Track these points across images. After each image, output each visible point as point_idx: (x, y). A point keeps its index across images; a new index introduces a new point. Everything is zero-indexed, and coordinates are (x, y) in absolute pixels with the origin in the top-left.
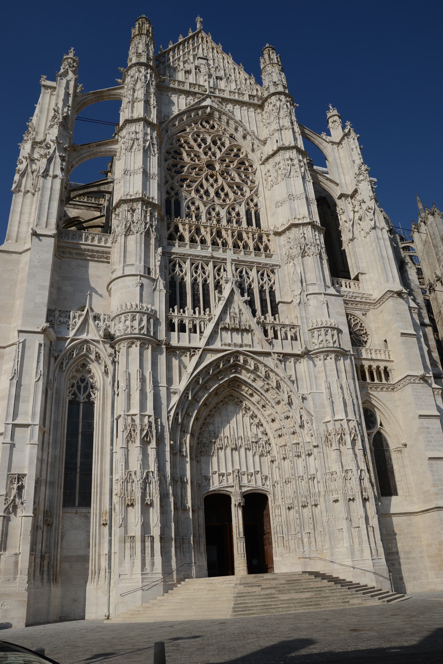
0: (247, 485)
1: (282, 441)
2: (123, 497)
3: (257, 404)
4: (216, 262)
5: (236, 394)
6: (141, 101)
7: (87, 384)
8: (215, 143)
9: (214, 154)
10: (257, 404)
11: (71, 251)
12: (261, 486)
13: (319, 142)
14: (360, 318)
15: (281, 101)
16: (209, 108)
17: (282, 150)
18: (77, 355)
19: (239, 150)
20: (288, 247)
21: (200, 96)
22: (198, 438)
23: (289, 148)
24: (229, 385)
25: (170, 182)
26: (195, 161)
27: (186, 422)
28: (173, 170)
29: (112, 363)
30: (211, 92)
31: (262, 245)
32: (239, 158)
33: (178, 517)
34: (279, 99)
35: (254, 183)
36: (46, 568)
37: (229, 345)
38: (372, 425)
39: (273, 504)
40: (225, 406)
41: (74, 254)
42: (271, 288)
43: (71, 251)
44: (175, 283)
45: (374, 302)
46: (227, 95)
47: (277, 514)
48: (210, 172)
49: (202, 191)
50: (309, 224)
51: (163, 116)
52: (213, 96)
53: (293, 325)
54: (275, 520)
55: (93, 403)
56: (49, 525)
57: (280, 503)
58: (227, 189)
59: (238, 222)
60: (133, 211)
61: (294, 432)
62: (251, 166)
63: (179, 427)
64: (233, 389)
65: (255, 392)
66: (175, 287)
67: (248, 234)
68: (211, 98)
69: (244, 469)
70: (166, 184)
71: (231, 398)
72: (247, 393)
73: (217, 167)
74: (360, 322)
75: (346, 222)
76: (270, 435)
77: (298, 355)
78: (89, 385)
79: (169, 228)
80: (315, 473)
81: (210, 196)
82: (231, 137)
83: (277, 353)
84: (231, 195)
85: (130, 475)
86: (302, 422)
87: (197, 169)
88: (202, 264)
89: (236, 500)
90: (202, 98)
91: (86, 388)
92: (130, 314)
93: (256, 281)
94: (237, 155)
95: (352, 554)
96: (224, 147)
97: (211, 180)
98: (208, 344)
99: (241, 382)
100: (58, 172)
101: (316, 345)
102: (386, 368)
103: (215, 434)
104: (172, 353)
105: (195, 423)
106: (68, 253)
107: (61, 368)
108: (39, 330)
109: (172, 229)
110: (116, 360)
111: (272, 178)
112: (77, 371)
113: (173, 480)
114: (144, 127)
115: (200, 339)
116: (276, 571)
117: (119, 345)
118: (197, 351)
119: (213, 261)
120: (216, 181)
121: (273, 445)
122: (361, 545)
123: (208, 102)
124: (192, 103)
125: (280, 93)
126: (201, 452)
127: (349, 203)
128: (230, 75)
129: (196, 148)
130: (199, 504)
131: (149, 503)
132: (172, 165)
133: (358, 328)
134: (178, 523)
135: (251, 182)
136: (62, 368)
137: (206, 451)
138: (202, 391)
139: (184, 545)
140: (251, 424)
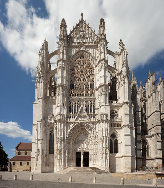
1: (92, 141)
8: (83, 63)
9: (83, 67)
19: (90, 64)
37: (81, 121)
42: (94, 105)
58: (86, 78)
69: (84, 147)
77: (96, 122)
84: (87, 79)
89: (82, 153)
94: (90, 66)
95: (102, 164)
98: (76, 121)
102: (120, 124)
109: (70, 92)
120: (83, 76)
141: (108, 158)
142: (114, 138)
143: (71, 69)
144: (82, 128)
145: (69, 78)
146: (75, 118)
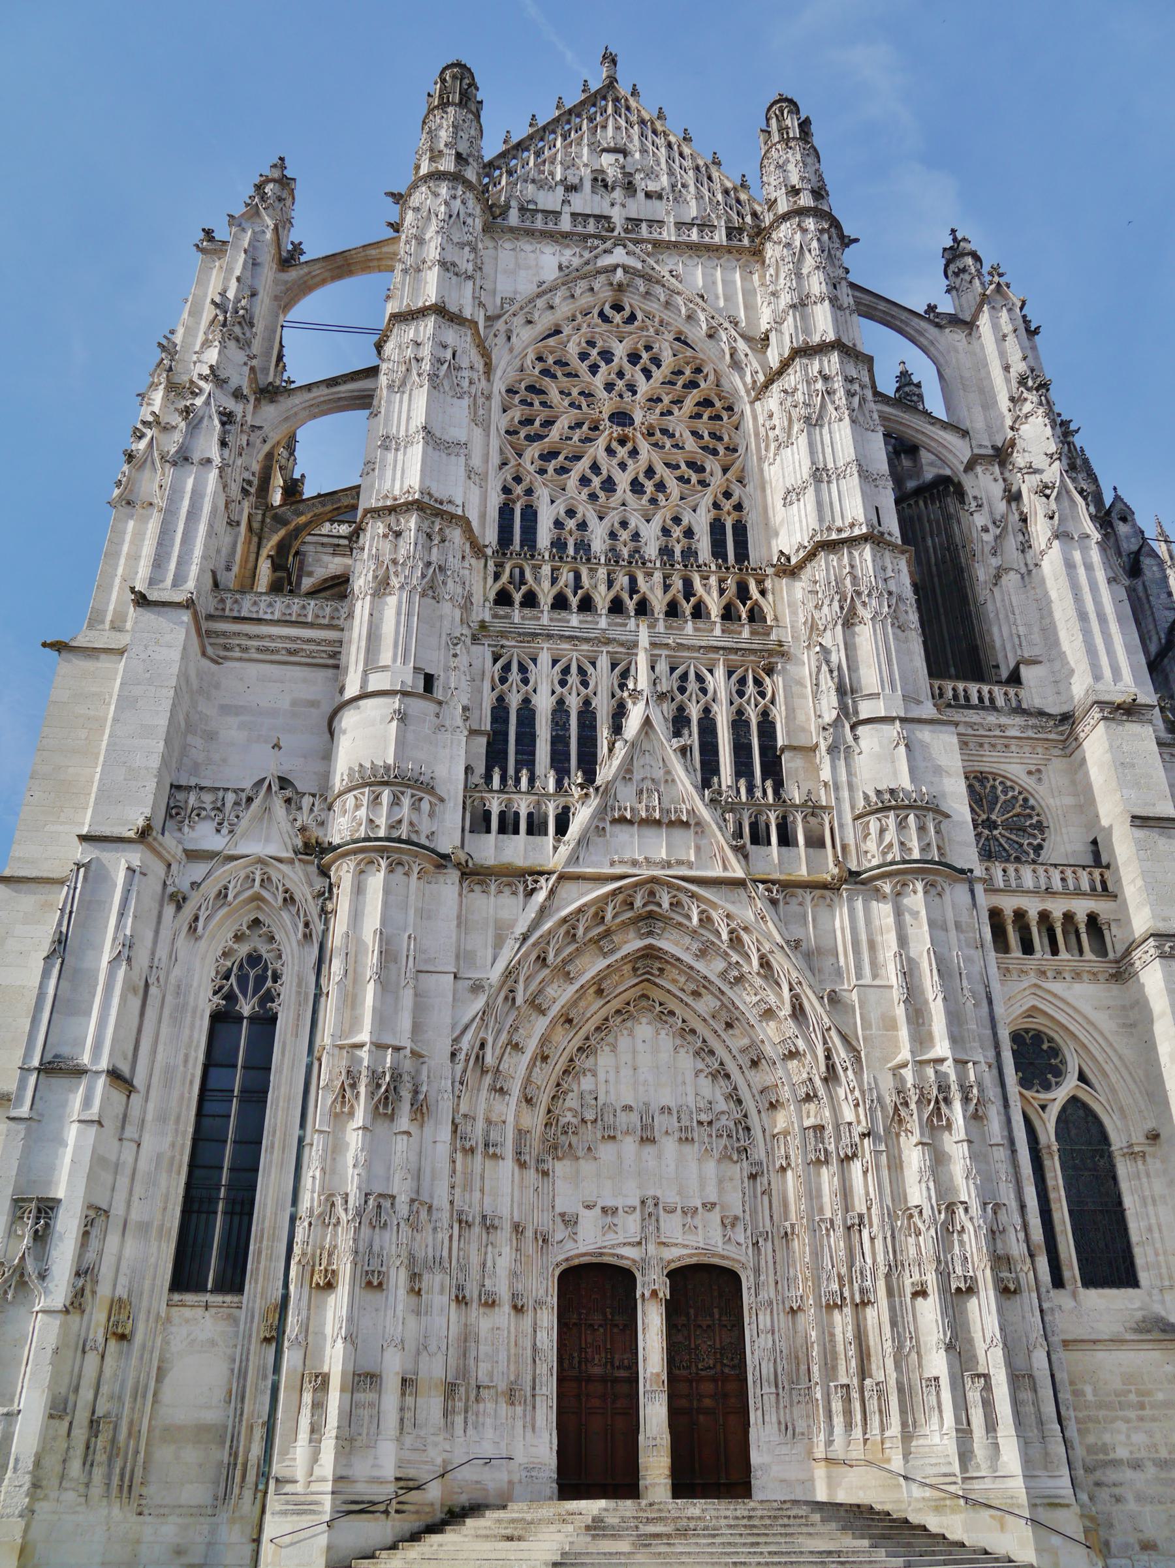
0: (680, 1241)
2: (309, 1267)
3: (711, 1021)
4: (616, 653)
5: (656, 994)
6: (434, 264)
7: (266, 969)
8: (634, 358)
9: (632, 388)
10: (711, 1021)
11: (243, 642)
12: (720, 1244)
13: (917, 331)
14: (1020, 782)
15: (804, 231)
16: (620, 271)
17: (801, 357)
18: (235, 897)
19: (698, 370)
20: (811, 605)
21: (596, 242)
22: (549, 1111)
23: (823, 348)
24: (635, 969)
25: (513, 463)
26: (579, 407)
27: (507, 1066)
28: (522, 435)
29: (320, 916)
30: (626, 231)
31: (744, 605)
32: (695, 391)
33: (466, 1325)
34: (799, 225)
35: (735, 450)
36: (101, 1457)
38: (1053, 1080)
39: (753, 1298)
40: (629, 1024)
41: (253, 650)
42: (765, 714)
43: (245, 642)
44: (506, 710)
45: (1062, 738)
46: (669, 235)
47: (761, 1327)
48: (617, 431)
49: (596, 481)
50: (865, 538)
51: (498, 301)
52: (630, 240)
53: (815, 807)
54: (756, 1344)
55: (273, 1019)
56: (123, 1337)
57: (773, 1295)
58: (661, 470)
59: (690, 554)
60: (398, 534)
61: (808, 1095)
62: (730, 409)
63: (488, 1079)
64: (648, 980)
65: (704, 987)
66: (506, 721)
67: (707, 578)
68: (625, 246)
70: (500, 469)
71: (644, 1003)
72: (683, 990)
73: (638, 417)
74: (1020, 793)
75: (986, 530)
76: (750, 1104)
77: (825, 886)
78: (269, 973)
79: (497, 576)
80: (865, 1211)
81: (615, 491)
82: (678, 339)
83: (763, 882)
84: (673, 486)
85: (333, 1204)
86: (831, 1068)
87: (585, 427)
88: (577, 659)
90: (602, 247)
91: (260, 980)
92: (367, 790)
93: (723, 696)
95: (965, 1455)
96: (659, 366)
97: (622, 452)
98: (574, 858)
99: (667, 962)
100: (214, 453)
101: (873, 857)
102: (1092, 919)
103: (596, 1099)
104: (477, 888)
105: (537, 1069)
106: (237, 649)
107: (192, 929)
108: (132, 834)
110: (330, 907)
111: (777, 431)
112: (238, 938)
113: (460, 1222)
114: (437, 327)
115: (555, 849)
116: (758, 1494)
117: (337, 870)
118: (542, 879)
119: (608, 652)
120: (634, 453)
121: (757, 1132)
122: (995, 1430)
123: (619, 256)
124: (576, 262)
125: (801, 212)
126: (555, 1147)
127: (996, 480)
128: (683, 186)
129: (586, 375)
130: (541, 1292)
131: (375, 1284)
132: (520, 422)
133: (1018, 810)
134: (465, 1341)
135: (727, 449)
136: (195, 930)
137: (570, 1145)
138: (555, 986)
139: (481, 1405)
140: (698, 1073)
141: (997, 1356)
142: (1047, 1087)
143: (511, 391)
144: (650, 954)
145: (495, 460)
146: (562, 827)
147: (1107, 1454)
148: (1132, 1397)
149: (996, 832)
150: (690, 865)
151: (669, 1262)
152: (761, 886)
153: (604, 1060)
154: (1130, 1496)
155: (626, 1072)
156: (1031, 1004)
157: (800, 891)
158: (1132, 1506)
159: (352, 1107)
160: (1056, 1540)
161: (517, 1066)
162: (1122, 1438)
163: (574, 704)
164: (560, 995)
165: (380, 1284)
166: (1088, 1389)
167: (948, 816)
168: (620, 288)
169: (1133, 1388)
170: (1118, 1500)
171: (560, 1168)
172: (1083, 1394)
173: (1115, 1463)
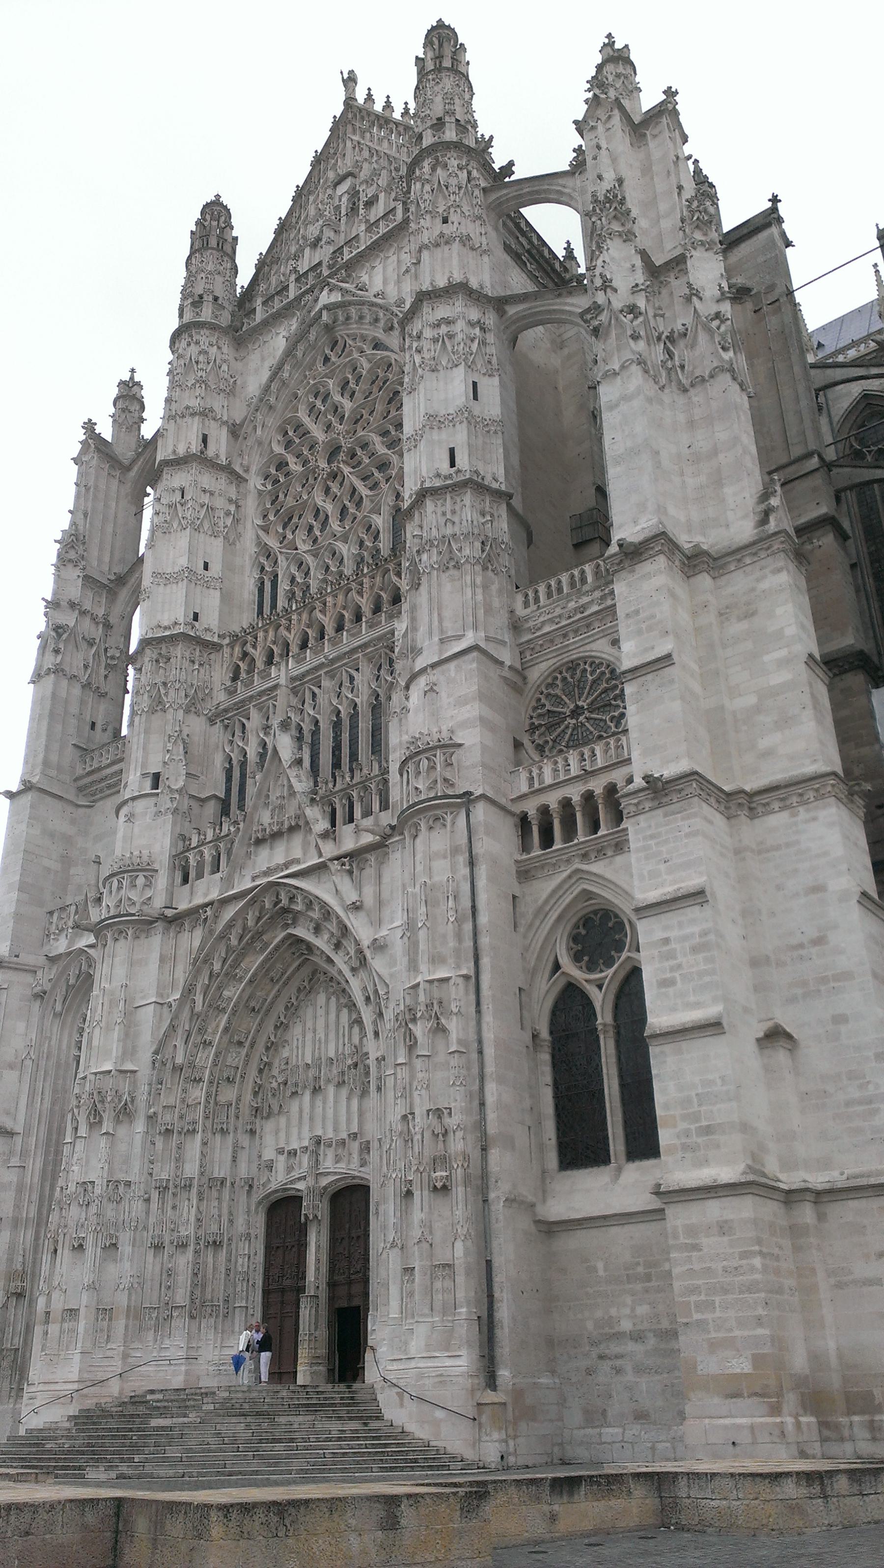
103: (287, 1063)
147: (612, 1328)
148: (640, 1269)
149: (581, 718)
150: (297, 861)
151: (325, 1188)
152: (336, 862)
153: (296, 1030)
154: (629, 1368)
155: (309, 1036)
156: (579, 889)
157: (368, 856)
158: (630, 1377)
159: (101, 1116)
160: (439, 1414)
161: (205, 1058)
162: (627, 1311)
163: (236, 757)
164: (233, 992)
165: (81, 1246)
166: (600, 1265)
167: (460, 745)
168: (329, 329)
169: (641, 1260)
170: (619, 1371)
171: (269, 1126)
172: (594, 1269)
173: (618, 1336)
